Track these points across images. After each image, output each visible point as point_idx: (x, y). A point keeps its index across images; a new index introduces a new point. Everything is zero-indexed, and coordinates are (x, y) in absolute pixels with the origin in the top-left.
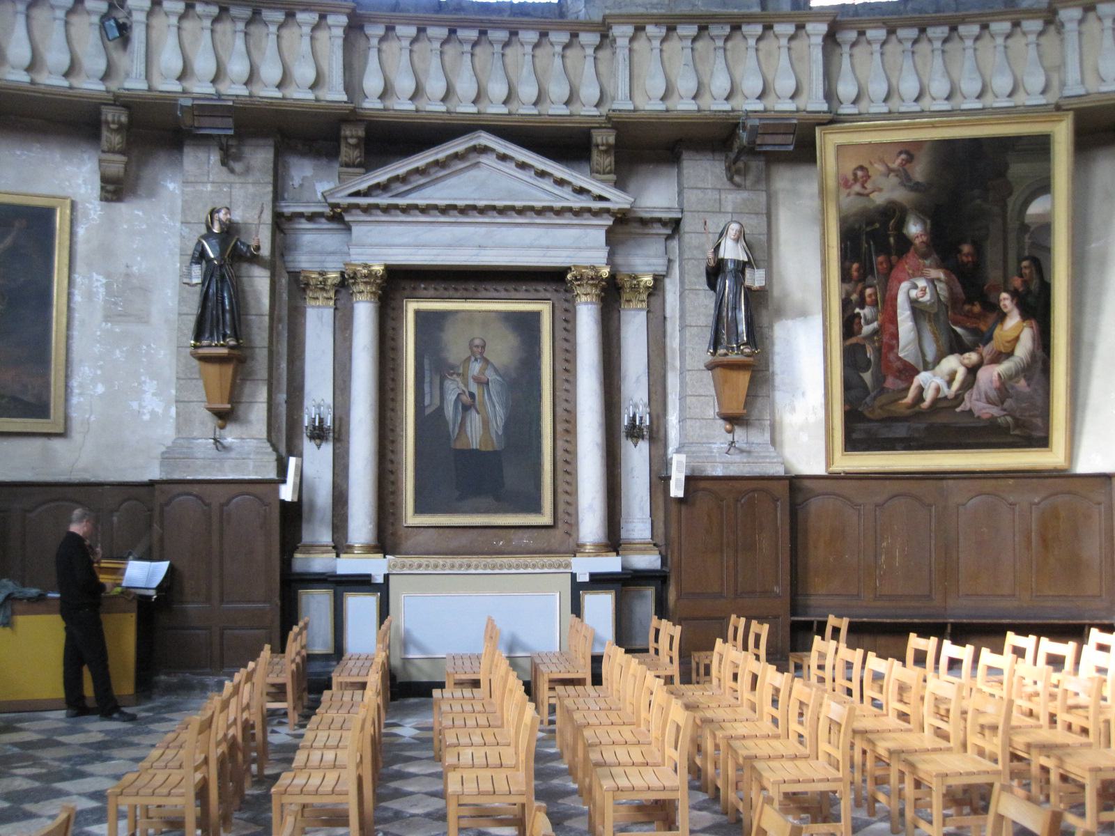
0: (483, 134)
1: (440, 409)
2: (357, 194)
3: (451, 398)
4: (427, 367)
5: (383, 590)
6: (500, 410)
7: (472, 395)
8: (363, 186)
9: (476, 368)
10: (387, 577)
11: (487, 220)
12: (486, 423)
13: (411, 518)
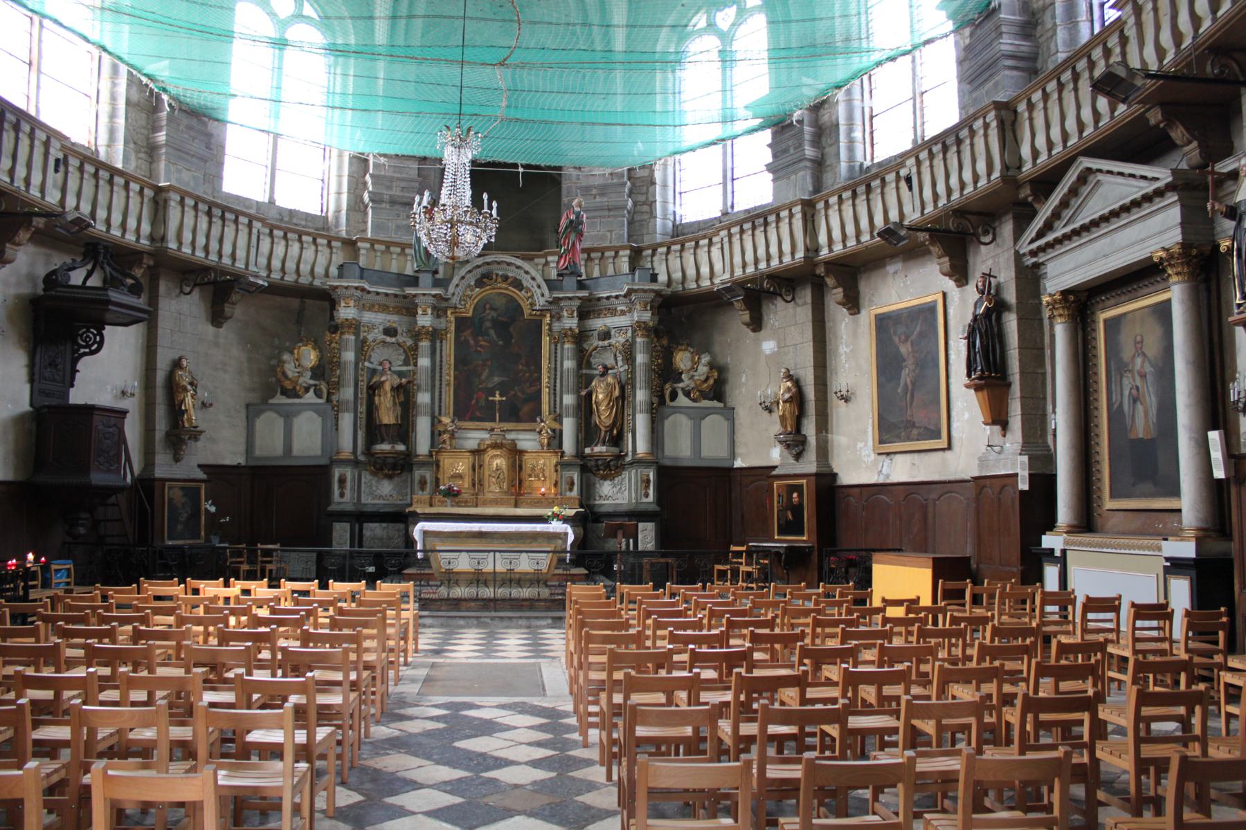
0: (1081, 159)
1: (1121, 405)
2: (1032, 241)
3: (1126, 393)
4: (1113, 368)
5: (1062, 561)
6: (1154, 399)
7: (1137, 388)
8: (1033, 235)
9: (1139, 361)
10: (1064, 552)
11: (1105, 231)
12: (1146, 413)
13: (1109, 504)
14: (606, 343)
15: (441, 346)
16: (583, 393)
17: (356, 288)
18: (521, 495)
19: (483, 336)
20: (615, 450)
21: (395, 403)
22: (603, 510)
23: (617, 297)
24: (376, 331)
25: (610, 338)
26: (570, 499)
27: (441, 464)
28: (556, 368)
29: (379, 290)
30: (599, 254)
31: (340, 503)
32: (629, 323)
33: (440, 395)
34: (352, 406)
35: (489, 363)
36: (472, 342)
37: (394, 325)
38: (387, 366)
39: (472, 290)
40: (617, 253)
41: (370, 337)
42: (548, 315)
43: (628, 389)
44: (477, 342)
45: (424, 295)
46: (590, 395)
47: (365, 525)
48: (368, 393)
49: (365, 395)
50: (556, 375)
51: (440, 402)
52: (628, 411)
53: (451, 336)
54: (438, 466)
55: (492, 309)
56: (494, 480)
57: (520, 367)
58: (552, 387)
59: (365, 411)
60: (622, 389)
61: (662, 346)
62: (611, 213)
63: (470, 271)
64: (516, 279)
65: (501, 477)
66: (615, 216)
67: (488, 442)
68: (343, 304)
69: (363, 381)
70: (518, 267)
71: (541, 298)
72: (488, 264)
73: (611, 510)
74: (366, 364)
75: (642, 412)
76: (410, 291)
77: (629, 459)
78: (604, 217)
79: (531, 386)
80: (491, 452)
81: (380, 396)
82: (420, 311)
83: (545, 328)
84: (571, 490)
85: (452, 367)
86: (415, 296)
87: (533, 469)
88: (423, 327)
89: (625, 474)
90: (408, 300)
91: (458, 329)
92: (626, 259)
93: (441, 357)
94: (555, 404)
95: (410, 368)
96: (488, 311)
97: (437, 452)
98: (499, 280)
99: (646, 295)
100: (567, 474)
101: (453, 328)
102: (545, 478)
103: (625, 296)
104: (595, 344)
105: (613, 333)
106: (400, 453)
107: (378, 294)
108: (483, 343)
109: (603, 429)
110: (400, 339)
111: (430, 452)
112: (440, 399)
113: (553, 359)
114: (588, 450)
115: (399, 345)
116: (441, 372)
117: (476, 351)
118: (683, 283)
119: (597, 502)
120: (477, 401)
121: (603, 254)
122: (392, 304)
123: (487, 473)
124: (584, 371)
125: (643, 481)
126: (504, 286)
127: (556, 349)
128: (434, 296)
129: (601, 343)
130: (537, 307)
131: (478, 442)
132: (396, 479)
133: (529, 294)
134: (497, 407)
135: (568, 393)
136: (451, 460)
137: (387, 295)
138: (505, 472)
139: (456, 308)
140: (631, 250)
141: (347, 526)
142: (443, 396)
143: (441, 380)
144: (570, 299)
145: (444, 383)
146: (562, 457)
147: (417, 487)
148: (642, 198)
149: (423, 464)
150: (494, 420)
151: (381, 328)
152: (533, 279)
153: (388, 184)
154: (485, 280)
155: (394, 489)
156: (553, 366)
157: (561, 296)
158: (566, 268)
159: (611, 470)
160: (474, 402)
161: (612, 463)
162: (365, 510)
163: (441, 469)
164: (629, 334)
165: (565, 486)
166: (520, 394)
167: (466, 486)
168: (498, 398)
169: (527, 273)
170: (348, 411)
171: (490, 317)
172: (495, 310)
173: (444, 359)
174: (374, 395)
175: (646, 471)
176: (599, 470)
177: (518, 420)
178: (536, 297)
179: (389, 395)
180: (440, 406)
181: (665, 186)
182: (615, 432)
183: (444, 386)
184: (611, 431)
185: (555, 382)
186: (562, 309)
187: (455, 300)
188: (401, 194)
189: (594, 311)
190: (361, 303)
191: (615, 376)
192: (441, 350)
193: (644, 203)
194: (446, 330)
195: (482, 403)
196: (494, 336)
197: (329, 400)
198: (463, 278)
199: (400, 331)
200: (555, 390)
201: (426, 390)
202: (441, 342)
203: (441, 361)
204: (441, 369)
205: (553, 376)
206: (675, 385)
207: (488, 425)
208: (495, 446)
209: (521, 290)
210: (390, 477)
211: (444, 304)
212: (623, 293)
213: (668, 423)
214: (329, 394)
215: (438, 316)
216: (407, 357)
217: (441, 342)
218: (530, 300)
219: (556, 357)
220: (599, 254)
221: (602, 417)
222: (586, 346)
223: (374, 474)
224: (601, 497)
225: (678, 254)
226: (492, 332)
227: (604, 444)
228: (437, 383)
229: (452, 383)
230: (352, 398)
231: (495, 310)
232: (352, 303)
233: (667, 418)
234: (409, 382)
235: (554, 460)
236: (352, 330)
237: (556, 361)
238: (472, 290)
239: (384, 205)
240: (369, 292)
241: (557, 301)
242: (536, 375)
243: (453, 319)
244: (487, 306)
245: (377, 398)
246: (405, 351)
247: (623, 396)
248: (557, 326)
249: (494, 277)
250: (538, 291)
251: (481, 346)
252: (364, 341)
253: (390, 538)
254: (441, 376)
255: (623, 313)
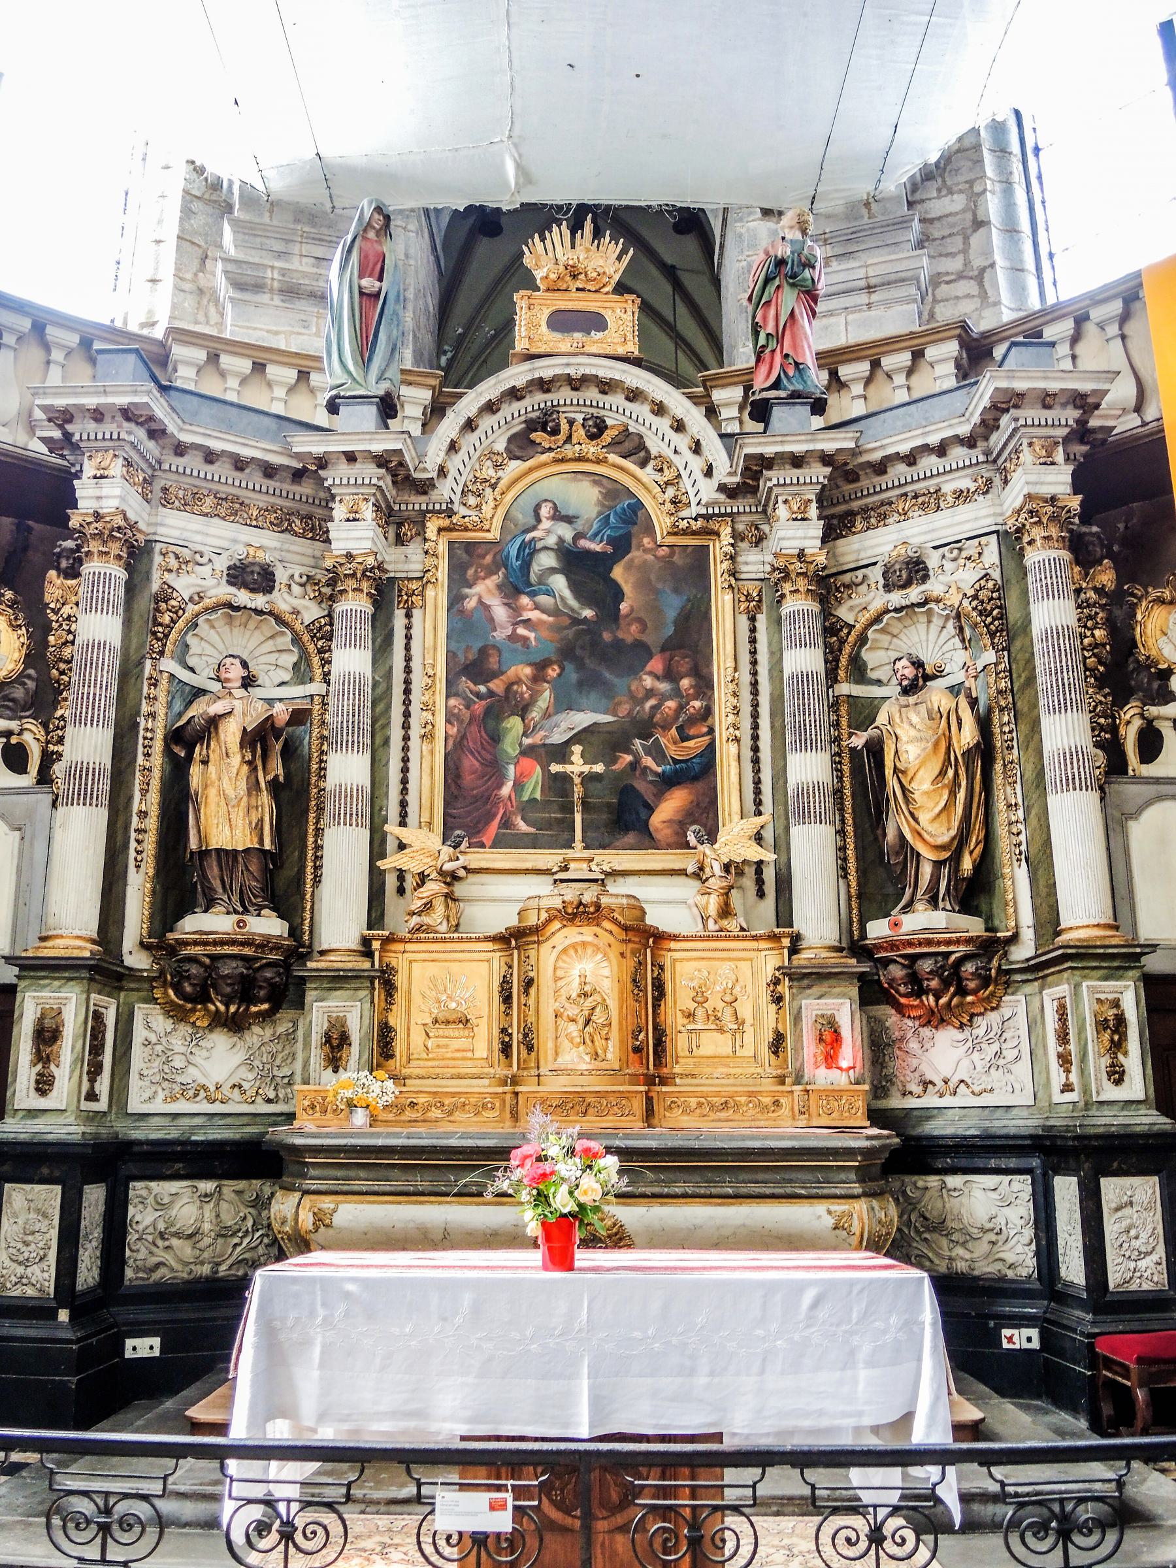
14: (914, 594)
15: (408, 628)
16: (859, 740)
17: (127, 414)
18: (664, 1081)
19: (532, 594)
20: (973, 926)
21: (254, 787)
22: (938, 1127)
23: (941, 450)
24: (206, 570)
25: (925, 578)
26: (834, 1094)
27: (400, 980)
28: (755, 684)
29: (216, 445)
30: (864, 367)
31: (32, 1113)
32: (986, 523)
33: (405, 770)
34: (105, 785)
35: (553, 672)
36: (500, 612)
37: (263, 557)
38: (235, 672)
39: (498, 466)
40: (918, 355)
41: (184, 585)
42: (726, 532)
43: (1001, 721)
44: (515, 609)
45: (351, 457)
46: (875, 749)
47: (138, 1188)
48: (168, 751)
49: (157, 760)
50: (755, 705)
51: (404, 791)
52: (1006, 793)
53: (437, 596)
54: (389, 988)
55: (558, 516)
56: (574, 1030)
57: (648, 682)
58: (747, 742)
59: (154, 811)
60: (984, 725)
61: (1100, 591)
62: (875, 297)
63: (490, 408)
64: (625, 432)
65: (599, 1017)
66: (888, 304)
67: (557, 903)
68: (89, 469)
69: (153, 715)
70: (634, 395)
71: (703, 483)
72: (543, 385)
73: (970, 1127)
74: (169, 665)
75: (1070, 783)
76: (310, 445)
77: (1023, 951)
78: (856, 308)
79: (685, 738)
80: (565, 936)
81: (205, 762)
82: (339, 511)
83: (718, 569)
84: (830, 1060)
85: (441, 686)
86: (322, 462)
87: (700, 997)
88: (350, 556)
89: (1015, 1005)
90: (306, 489)
91: (459, 578)
92: (950, 368)
93: (408, 659)
94: (758, 792)
95: (316, 687)
96: (546, 524)
97: (388, 941)
98: (580, 433)
99: (1050, 415)
100: (813, 1006)
101: (443, 574)
102: (740, 1022)
103: (970, 442)
104: (876, 605)
105: (933, 560)
106: (265, 944)
107: (210, 457)
108: (534, 615)
109: (927, 853)
110: (282, 600)
111: (366, 942)
112: (405, 781)
113: (745, 658)
114: (878, 929)
115: (279, 620)
116: (407, 703)
117: (514, 637)
118: (1138, 409)
119: (912, 1103)
120: (518, 786)
121: (876, 364)
122: (263, 501)
123: (548, 1007)
124: (845, 688)
125: (1102, 1025)
126: (591, 449)
127: (753, 630)
128: (381, 461)
129: (896, 598)
130: (694, 510)
131: (517, 907)
132: (257, 1034)
133: (668, 474)
134: (578, 791)
135: (804, 744)
136: (433, 969)
137: (239, 464)
138: (613, 1004)
139: (450, 513)
140: (963, 344)
141: (50, 1196)
142: (413, 775)
143: (406, 726)
144: (797, 461)
145: (415, 732)
146: (794, 950)
147: (317, 1055)
148: (955, 265)
149: (338, 980)
150: (569, 844)
151: (222, 564)
152: (679, 426)
153: (278, 246)
154: (537, 436)
155: (248, 1063)
156: (745, 677)
157: (769, 450)
158: (776, 385)
159: (962, 991)
160: (506, 790)
161: (969, 967)
162: (137, 1134)
163: (399, 996)
164: (991, 555)
165: (810, 1049)
166: (648, 761)
167: (481, 1051)
168: (577, 766)
169: (660, 409)
170: (84, 797)
171: (551, 541)
172: (569, 520)
173: (416, 665)
174: (189, 758)
175: (1109, 988)
176: (919, 991)
177: (648, 841)
178: (686, 483)
179: (236, 759)
180: (403, 804)
181: (1011, 230)
182: (967, 864)
183: (414, 743)
184: (956, 858)
185: (755, 727)
186: (765, 512)
187: (445, 490)
188: (315, 270)
189: (865, 510)
190: (158, 485)
191: (954, 690)
192: (408, 638)
193: (961, 276)
194: (424, 579)
195: (534, 788)
196: (567, 594)
197: (44, 778)
198: (470, 425)
199: (281, 576)
200: (755, 749)
201: (358, 747)
202: (408, 616)
203: (408, 670)
204: (407, 692)
205: (746, 709)
206: (1153, 711)
207: (549, 858)
208: (578, 914)
209: (643, 464)
210: (235, 1025)
211: (418, 502)
212: (964, 430)
213: (1140, 832)
214: (49, 759)
215: (400, 541)
216: (304, 656)
217: (408, 616)
218: (671, 492)
219: (754, 652)
220: (864, 367)
221: (924, 817)
222: (844, 613)
223: (177, 1014)
224: (926, 1084)
225: (1113, 330)
226: (559, 583)
227: (933, 902)
228: (396, 734)
229: (440, 733)
230: (104, 757)
231: (569, 520)
232: (117, 468)
233: (1136, 814)
234: (299, 717)
235: (769, 961)
236: (115, 548)
237: (754, 663)
238: (498, 466)
239: (265, 298)
240: (180, 449)
241: (757, 466)
242: (697, 704)
243: (443, 548)
244: (545, 511)
245: (195, 770)
246: (297, 640)
247: (985, 751)
248: (754, 563)
249: (564, 426)
250: (697, 464)
251: (527, 623)
252: (164, 596)
253: (224, 1233)
254: (407, 715)
255: (961, 496)
